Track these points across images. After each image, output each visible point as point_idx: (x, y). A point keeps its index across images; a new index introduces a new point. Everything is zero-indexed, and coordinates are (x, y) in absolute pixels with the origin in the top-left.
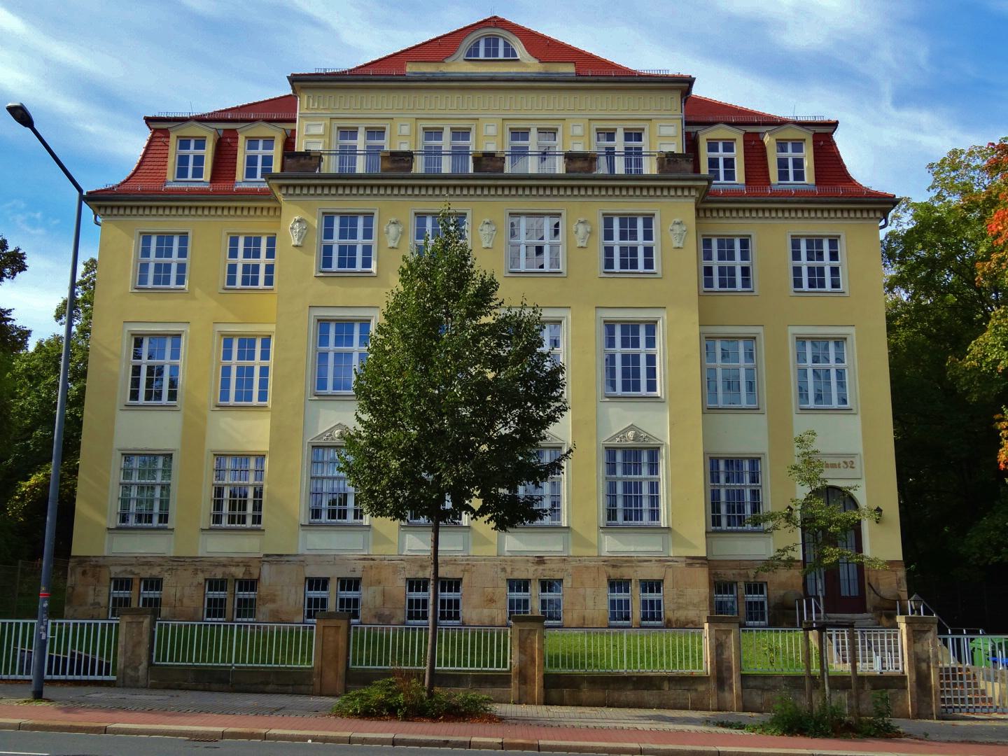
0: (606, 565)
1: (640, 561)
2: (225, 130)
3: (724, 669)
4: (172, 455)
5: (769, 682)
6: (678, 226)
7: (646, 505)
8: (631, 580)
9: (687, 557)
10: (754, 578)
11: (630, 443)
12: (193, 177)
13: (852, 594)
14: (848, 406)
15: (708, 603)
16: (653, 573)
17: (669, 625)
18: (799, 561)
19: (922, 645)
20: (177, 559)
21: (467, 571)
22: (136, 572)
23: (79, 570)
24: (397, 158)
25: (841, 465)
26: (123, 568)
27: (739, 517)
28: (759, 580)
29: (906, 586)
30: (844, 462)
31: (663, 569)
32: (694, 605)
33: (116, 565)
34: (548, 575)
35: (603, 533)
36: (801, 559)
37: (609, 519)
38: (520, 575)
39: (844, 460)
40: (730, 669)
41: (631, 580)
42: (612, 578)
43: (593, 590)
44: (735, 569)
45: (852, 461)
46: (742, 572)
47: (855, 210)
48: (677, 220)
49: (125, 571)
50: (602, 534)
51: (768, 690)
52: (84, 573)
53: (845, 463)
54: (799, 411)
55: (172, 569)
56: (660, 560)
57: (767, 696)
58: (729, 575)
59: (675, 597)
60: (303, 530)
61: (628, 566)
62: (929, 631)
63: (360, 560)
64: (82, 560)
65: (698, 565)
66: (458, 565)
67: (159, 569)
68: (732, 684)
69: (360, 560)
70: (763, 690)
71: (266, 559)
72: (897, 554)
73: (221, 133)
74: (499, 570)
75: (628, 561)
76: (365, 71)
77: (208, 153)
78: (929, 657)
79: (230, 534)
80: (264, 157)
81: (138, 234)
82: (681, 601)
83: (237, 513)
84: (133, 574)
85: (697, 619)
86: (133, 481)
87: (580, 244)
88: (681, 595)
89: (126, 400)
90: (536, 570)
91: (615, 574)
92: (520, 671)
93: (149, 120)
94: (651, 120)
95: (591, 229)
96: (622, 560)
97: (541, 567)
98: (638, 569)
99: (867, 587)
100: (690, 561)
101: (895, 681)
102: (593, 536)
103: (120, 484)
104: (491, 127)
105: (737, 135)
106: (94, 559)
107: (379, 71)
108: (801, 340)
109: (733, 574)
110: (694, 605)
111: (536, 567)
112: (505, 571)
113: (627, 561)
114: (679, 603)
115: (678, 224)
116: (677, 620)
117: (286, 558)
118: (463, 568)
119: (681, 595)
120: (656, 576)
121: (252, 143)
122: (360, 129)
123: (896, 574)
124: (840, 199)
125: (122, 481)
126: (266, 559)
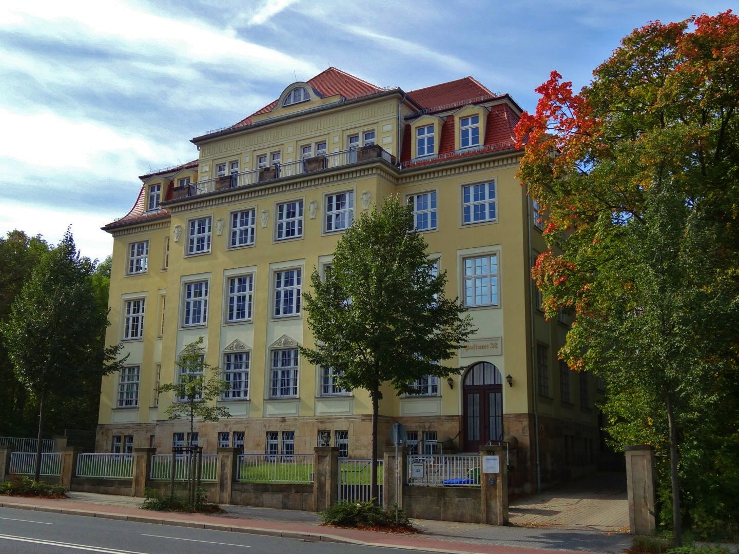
2: (492, 107)
3: (224, 479)
4: (139, 366)
5: (244, 486)
6: (365, 195)
9: (363, 415)
10: (429, 428)
11: (235, 350)
12: (428, 153)
16: (341, 426)
17: (350, 458)
19: (323, 465)
20: (140, 425)
21: (247, 427)
22: (123, 432)
24: (223, 181)
25: (489, 347)
27: (288, 389)
28: (432, 430)
29: (528, 432)
33: (115, 428)
35: (318, 401)
40: (227, 479)
42: (320, 429)
44: (417, 422)
46: (421, 424)
47: (503, 160)
48: (364, 191)
50: (317, 402)
51: (244, 492)
52: (102, 433)
55: (137, 430)
56: (347, 418)
57: (244, 495)
58: (413, 427)
59: (354, 441)
62: (327, 456)
63: (198, 422)
65: (368, 420)
67: (131, 430)
68: (227, 488)
69: (198, 422)
70: (242, 492)
71: (159, 423)
72: (524, 409)
73: (490, 109)
75: (330, 419)
76: (239, 126)
77: (481, 125)
78: (326, 473)
80: (428, 139)
81: (461, 187)
82: (357, 444)
84: (121, 433)
86: (134, 382)
87: (311, 217)
89: (122, 337)
90: (281, 425)
91: (322, 427)
92: (136, 479)
93: (141, 178)
94: (378, 123)
95: (318, 206)
96: (326, 418)
97: (283, 424)
98: (335, 424)
100: (363, 418)
101: (308, 488)
102: (311, 402)
103: (120, 384)
104: (290, 148)
105: (480, 111)
106: (107, 426)
107: (263, 119)
108: (464, 259)
109: (416, 426)
110: (365, 447)
111: (281, 424)
112: (266, 427)
113: (329, 419)
115: (365, 194)
118: (245, 425)
120: (344, 429)
121: (464, 121)
122: (359, 133)
123: (522, 424)
124: (493, 153)
125: (120, 382)
126: (159, 423)
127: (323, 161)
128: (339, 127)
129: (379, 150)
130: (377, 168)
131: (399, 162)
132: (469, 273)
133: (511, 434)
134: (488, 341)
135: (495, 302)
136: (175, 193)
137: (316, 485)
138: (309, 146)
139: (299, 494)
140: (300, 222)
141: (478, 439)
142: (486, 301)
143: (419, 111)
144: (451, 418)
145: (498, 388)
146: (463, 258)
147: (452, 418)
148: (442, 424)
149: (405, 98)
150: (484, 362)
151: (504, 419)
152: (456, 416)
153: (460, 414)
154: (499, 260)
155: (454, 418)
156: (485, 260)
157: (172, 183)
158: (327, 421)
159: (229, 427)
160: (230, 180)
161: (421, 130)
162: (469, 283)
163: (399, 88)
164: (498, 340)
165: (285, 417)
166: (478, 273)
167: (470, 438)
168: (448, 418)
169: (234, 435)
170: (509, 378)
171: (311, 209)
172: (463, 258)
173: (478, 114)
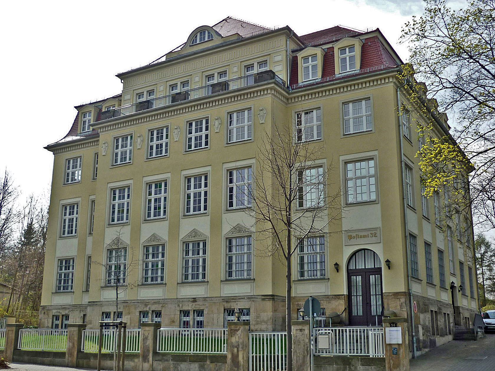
0: (224, 302)
1: (239, 299)
23: (43, 312)
24: (142, 105)
25: (369, 236)
26: (56, 311)
31: (250, 302)
34: (197, 308)
38: (185, 308)
39: (371, 232)
42: (226, 308)
49: (57, 312)
52: (44, 313)
61: (234, 301)
62: (239, 330)
64: (44, 307)
65: (267, 300)
66: (160, 304)
69: (122, 303)
74: (177, 306)
75: (235, 299)
82: (258, 320)
83: (66, 285)
90: (192, 305)
91: (228, 306)
98: (238, 303)
100: (264, 297)
106: (48, 307)
108: (346, 163)
112: (179, 306)
113: (233, 299)
114: (257, 321)
115: (262, 110)
117: (96, 303)
119: (258, 316)
126: (89, 304)
127: (224, 85)
128: (238, 59)
129: (271, 74)
130: (271, 89)
131: (289, 85)
132: (350, 175)
133: (391, 309)
134: (368, 231)
135: (373, 197)
136: (102, 116)
137: (229, 356)
138: (212, 76)
139: (214, 364)
140: (207, 136)
141: (361, 314)
142: (365, 198)
143: (303, 46)
145: (378, 271)
146: (345, 163)
149: (292, 34)
150: (364, 249)
151: (384, 297)
152: (343, 295)
153: (345, 294)
154: (375, 164)
155: (340, 297)
156: (363, 163)
157: (101, 110)
158: (232, 301)
159: (149, 306)
160: (148, 104)
161: (306, 59)
162: (350, 184)
163: (287, 26)
165: (195, 298)
166: (358, 174)
167: (354, 313)
169: (194, 313)
170: (388, 261)
171: (216, 124)
172: (345, 163)
173: (354, 45)
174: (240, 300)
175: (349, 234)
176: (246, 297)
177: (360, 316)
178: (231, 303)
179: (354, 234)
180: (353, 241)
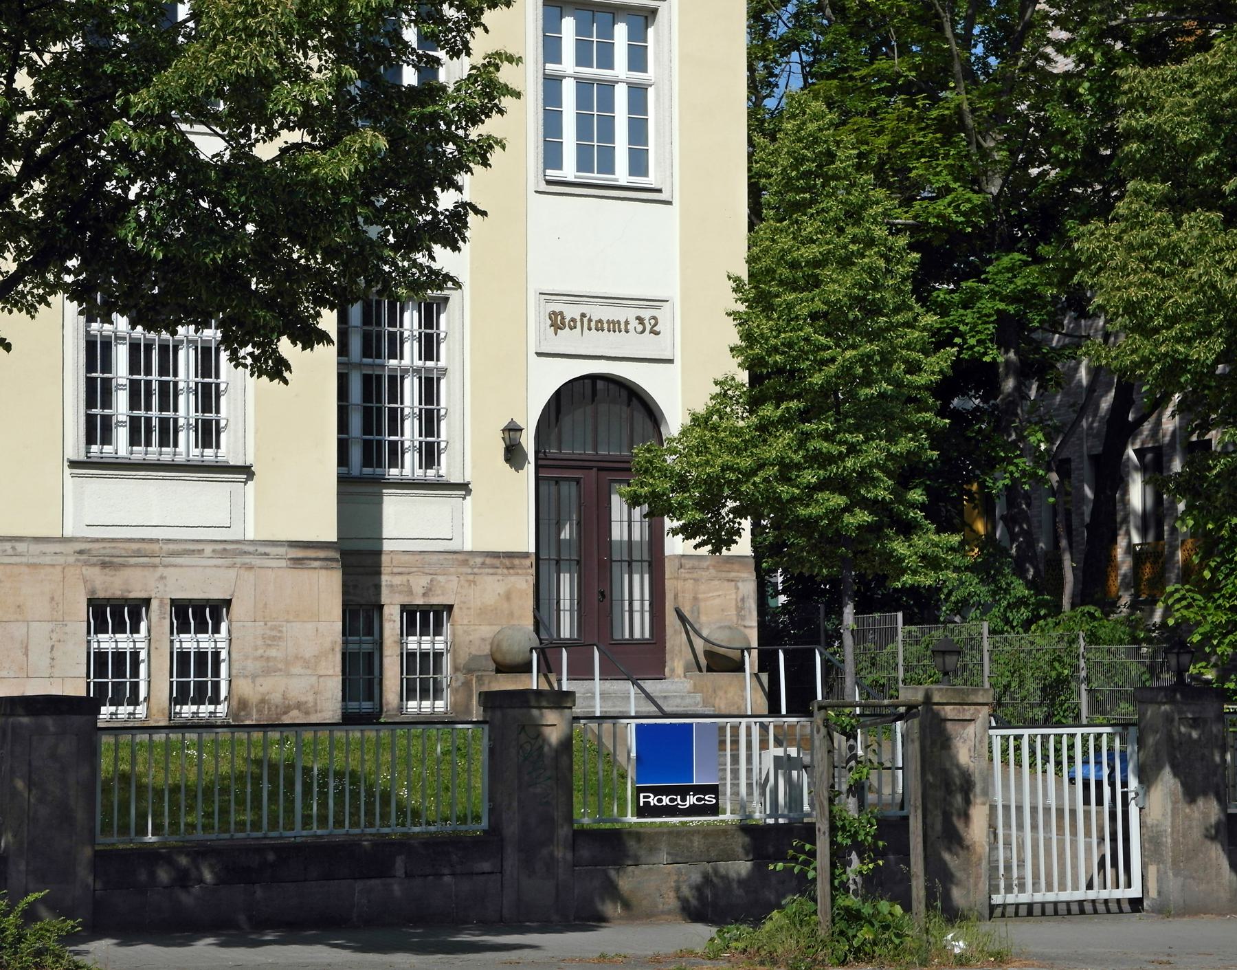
0: (86, 563)
7: (186, 409)
8: (147, 602)
10: (424, 594)
13: (637, 635)
14: (651, 180)
15: (339, 657)
18: (525, 555)
25: (630, 327)
29: (755, 614)
30: (638, 318)
31: (232, 573)
32: (307, 664)
36: (532, 549)
37: (90, 440)
41: (147, 602)
42: (101, 594)
43: (50, 626)
45: (654, 318)
53: (640, 320)
54: (543, 187)
59: (260, 642)
60: (73, 476)
65: (317, 564)
79: (436, 496)
82: (273, 652)
85: (310, 698)
88: (273, 640)
91: (113, 585)
98: (168, 572)
99: (671, 619)
100: (299, 553)
110: (307, 664)
113: (138, 553)
114: (268, 659)
116: (263, 701)
119: (273, 638)
123: (737, 588)
144: (509, 558)
147: (507, 562)
148: (474, 582)
155: (517, 561)
158: (133, 561)
164: (658, 308)
168: (496, 562)
174: (179, 561)
175: (557, 308)
176: (208, 549)
177: (642, 643)
178: (126, 573)
179: (571, 312)
180: (568, 341)
